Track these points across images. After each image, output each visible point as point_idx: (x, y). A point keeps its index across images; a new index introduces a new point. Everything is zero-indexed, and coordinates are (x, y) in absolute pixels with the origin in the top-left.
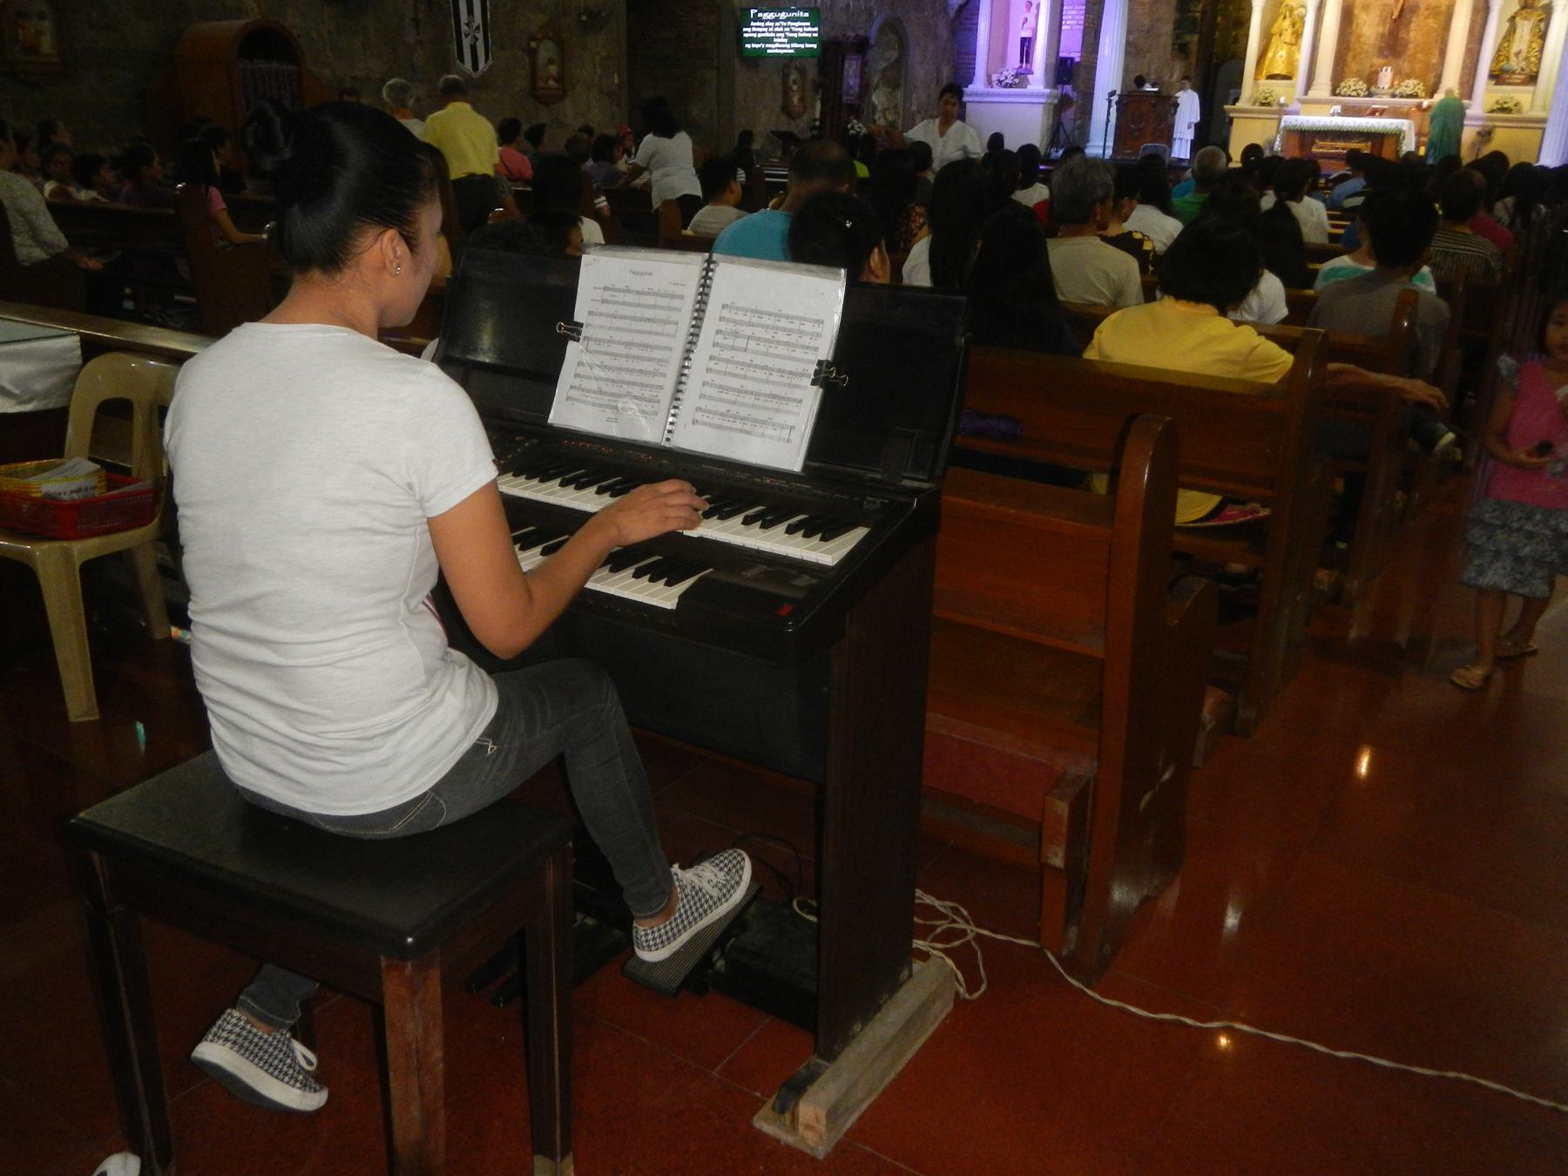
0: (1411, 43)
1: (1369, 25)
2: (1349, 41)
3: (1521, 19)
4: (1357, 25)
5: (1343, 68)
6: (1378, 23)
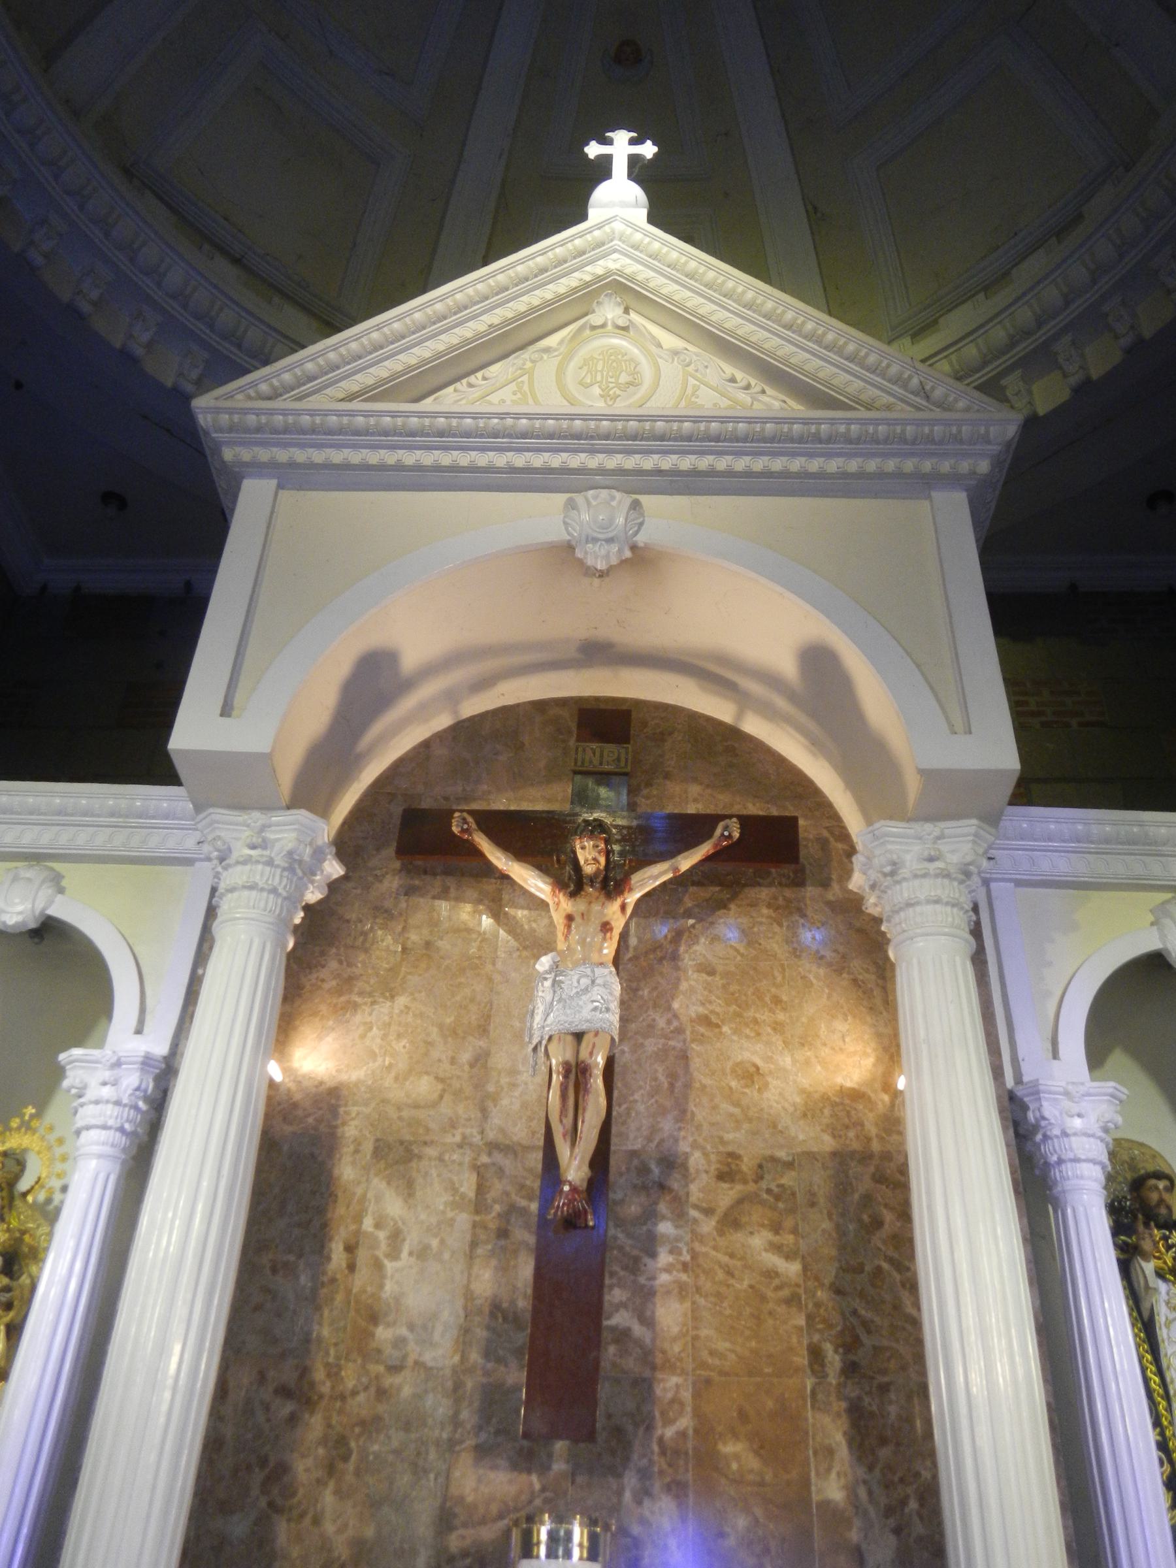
0: (670, 1366)
1: (422, 1253)
2: (307, 1341)
3: (1160, 1274)
4: (350, 1249)
5: (263, 1523)
6: (474, 1245)
